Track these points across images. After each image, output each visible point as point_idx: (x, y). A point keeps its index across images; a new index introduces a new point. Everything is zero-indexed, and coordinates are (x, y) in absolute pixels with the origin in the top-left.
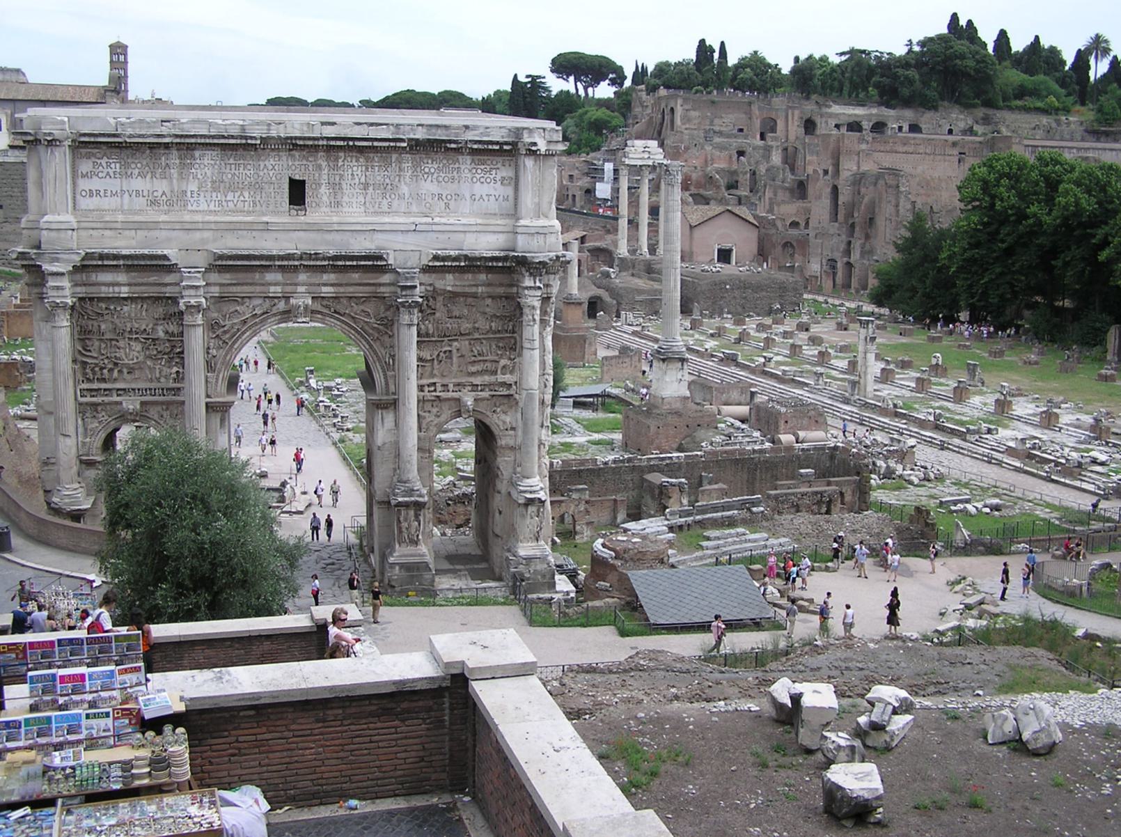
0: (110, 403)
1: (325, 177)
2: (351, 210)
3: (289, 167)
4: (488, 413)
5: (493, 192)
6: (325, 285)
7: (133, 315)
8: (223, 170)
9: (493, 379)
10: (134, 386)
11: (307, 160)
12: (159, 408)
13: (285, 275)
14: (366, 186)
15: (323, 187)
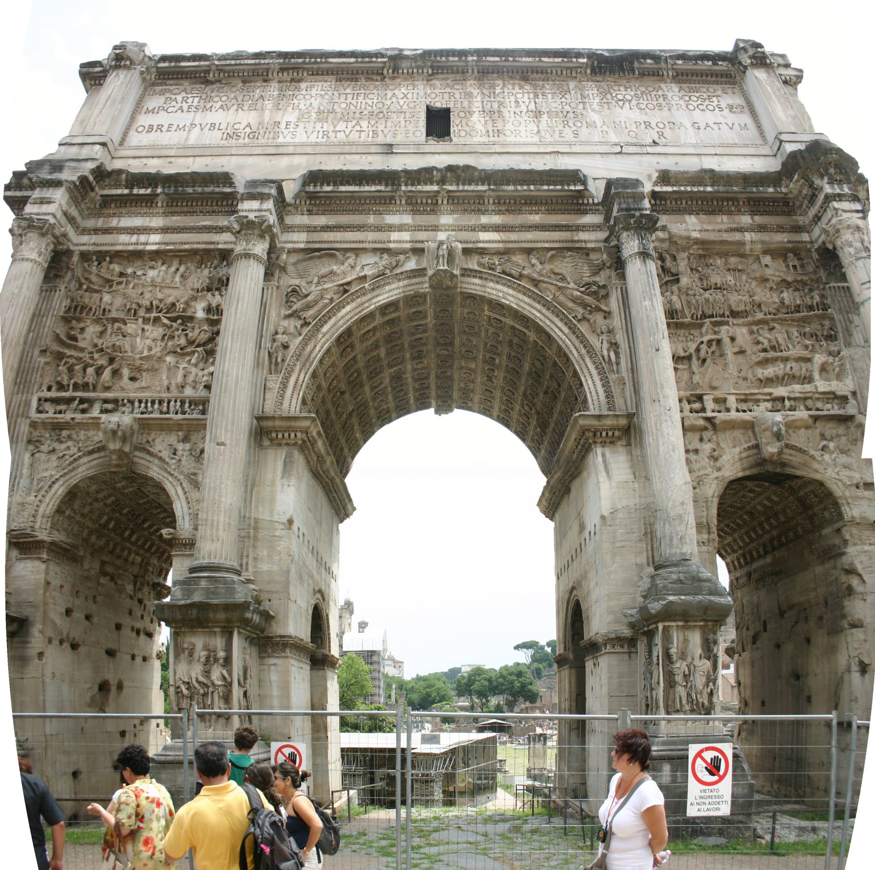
0: (82, 425)
1: (480, 104)
2: (518, 139)
3: (426, 95)
4: (817, 454)
5: (721, 120)
6: (485, 228)
7: (159, 280)
8: (336, 100)
9: (808, 387)
10: (132, 395)
11: (452, 87)
12: (172, 439)
13: (418, 217)
14: (538, 114)
15: (475, 117)
